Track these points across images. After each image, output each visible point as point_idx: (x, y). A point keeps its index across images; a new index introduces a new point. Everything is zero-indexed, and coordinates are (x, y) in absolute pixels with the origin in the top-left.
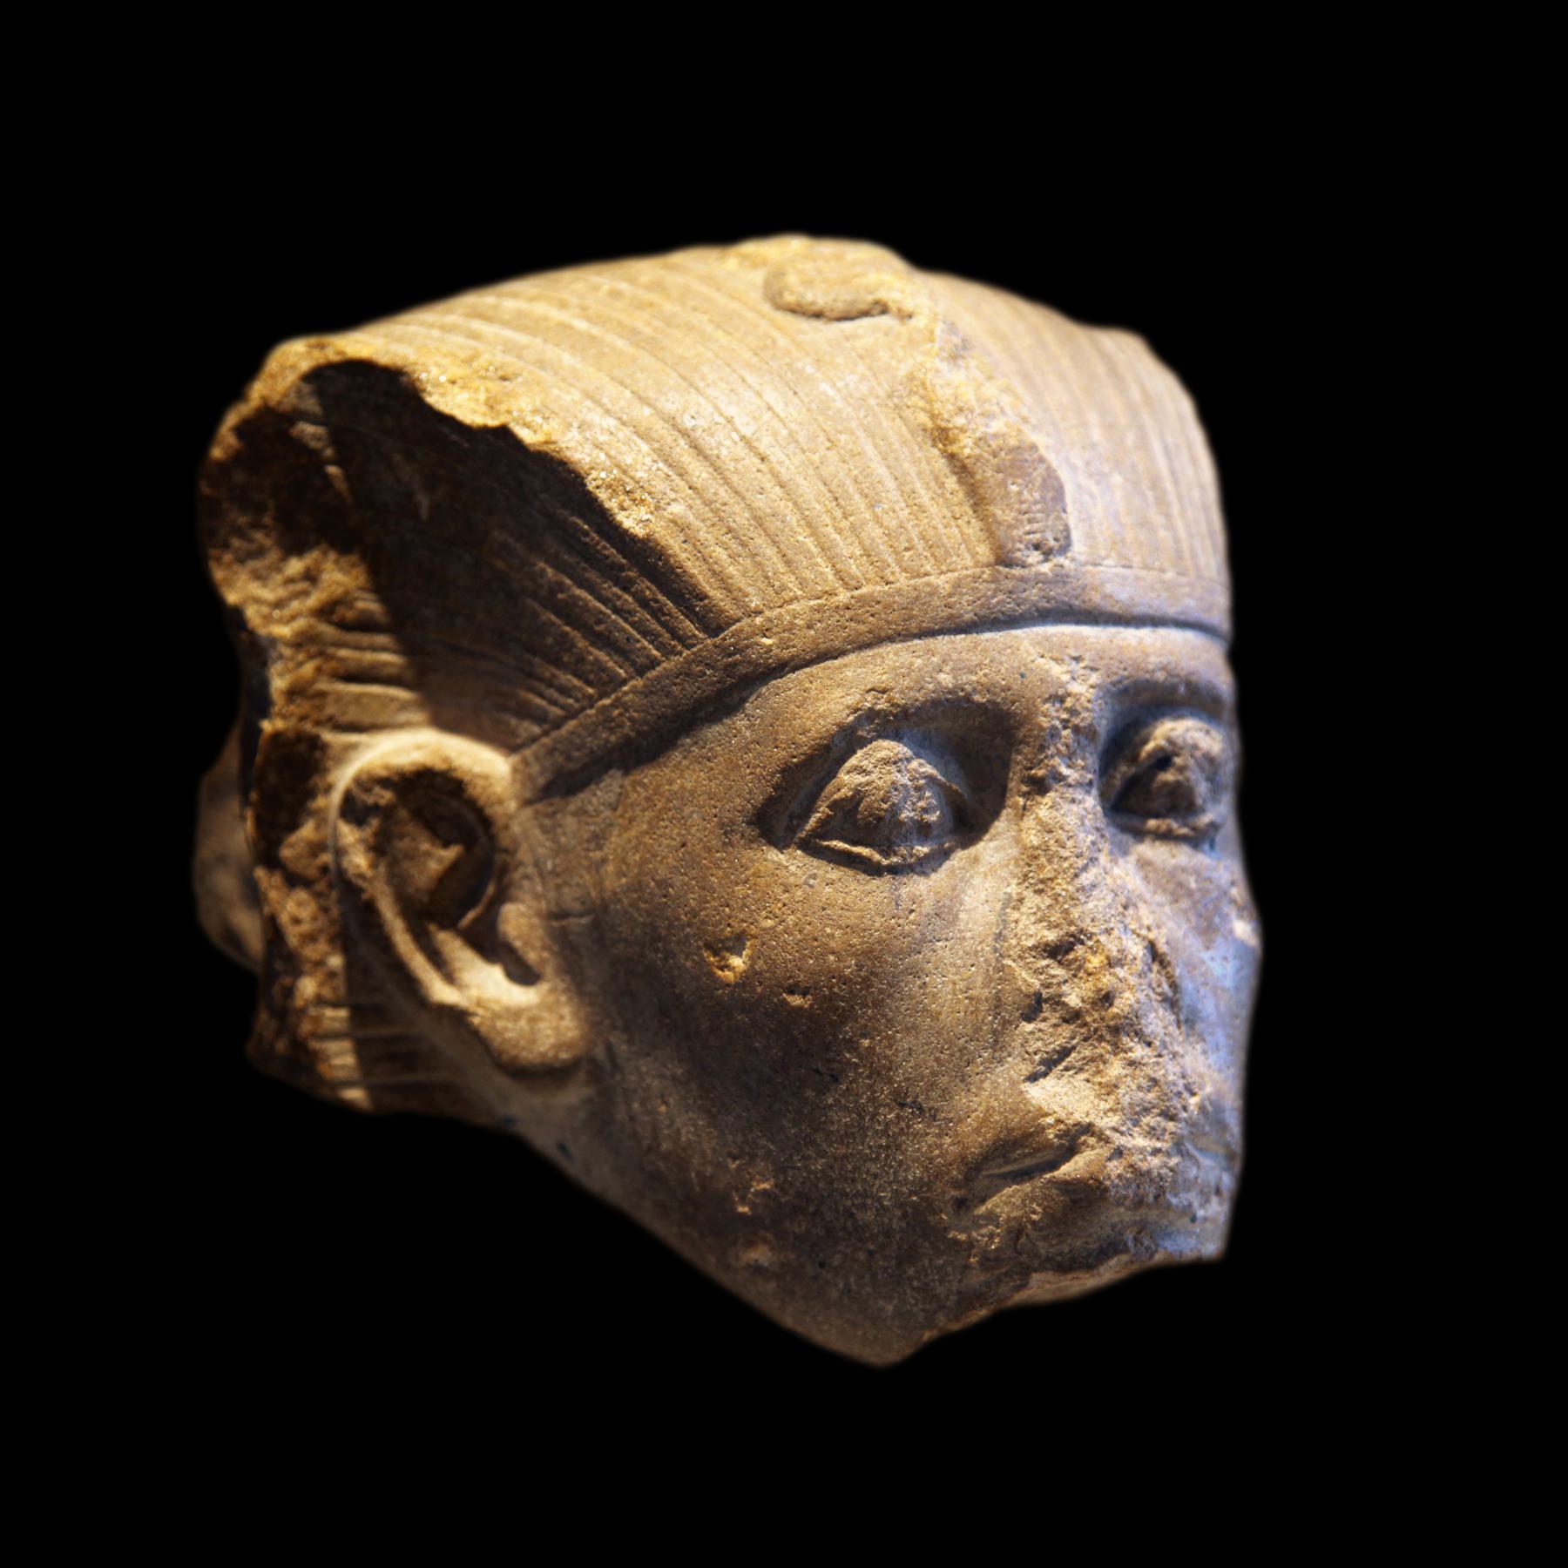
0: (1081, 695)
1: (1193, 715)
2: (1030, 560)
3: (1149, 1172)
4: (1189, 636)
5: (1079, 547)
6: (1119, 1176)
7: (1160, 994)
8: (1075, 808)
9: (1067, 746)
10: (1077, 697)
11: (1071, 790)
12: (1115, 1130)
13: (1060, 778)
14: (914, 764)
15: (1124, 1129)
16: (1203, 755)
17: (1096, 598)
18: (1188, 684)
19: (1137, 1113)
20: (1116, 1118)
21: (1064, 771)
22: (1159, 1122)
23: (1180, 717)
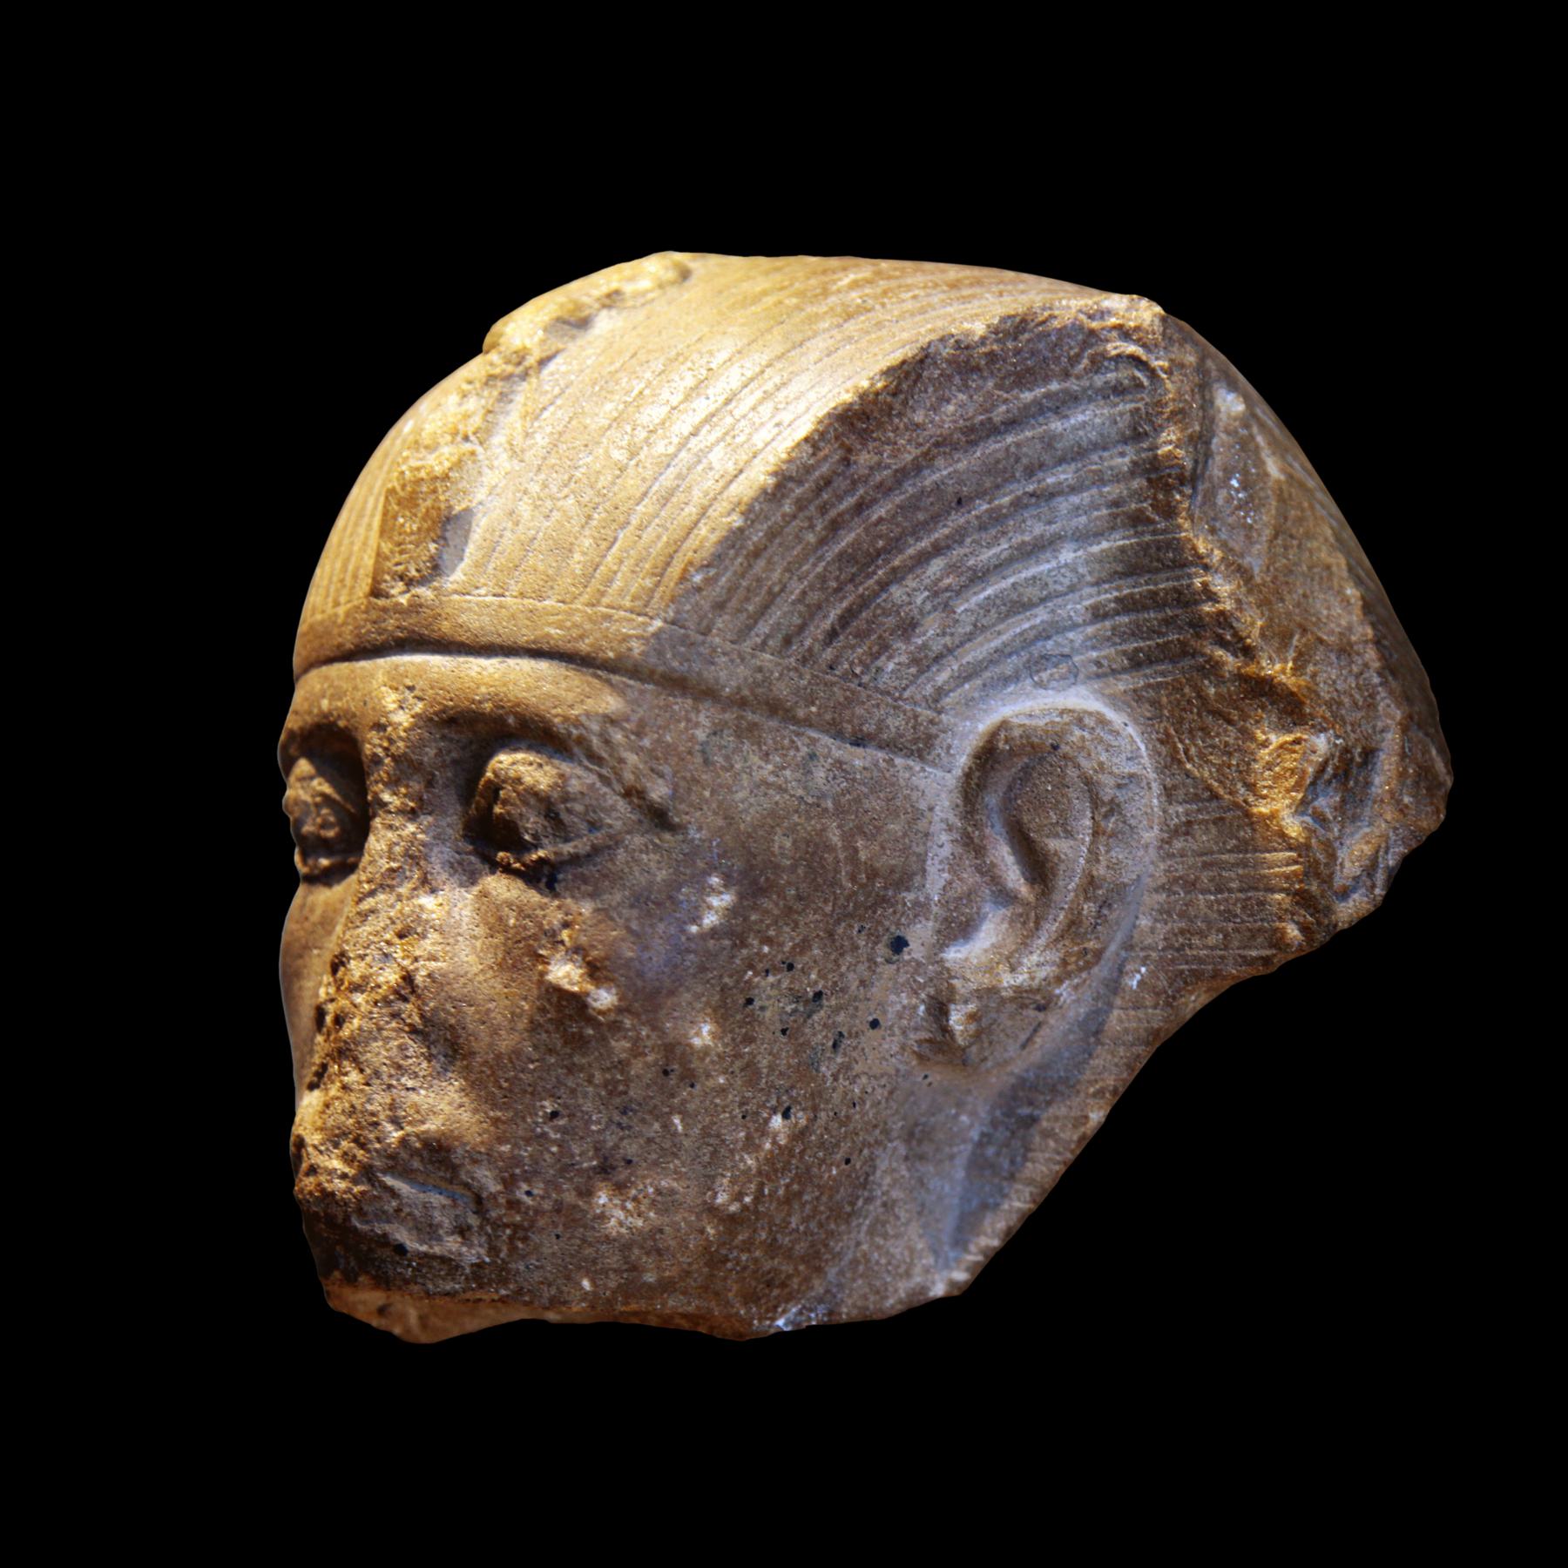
0: (400, 724)
1: (530, 748)
2: (393, 592)
3: (332, 1194)
4: (543, 666)
5: (457, 577)
6: (311, 1193)
7: (410, 1025)
8: (390, 834)
9: (388, 774)
10: (396, 726)
11: (390, 816)
12: (315, 1147)
13: (384, 805)
14: (315, 783)
15: (322, 1148)
16: (525, 790)
17: (445, 627)
18: (516, 714)
19: (337, 1136)
20: (319, 1137)
21: (386, 797)
22: (351, 1148)
23: (516, 750)
